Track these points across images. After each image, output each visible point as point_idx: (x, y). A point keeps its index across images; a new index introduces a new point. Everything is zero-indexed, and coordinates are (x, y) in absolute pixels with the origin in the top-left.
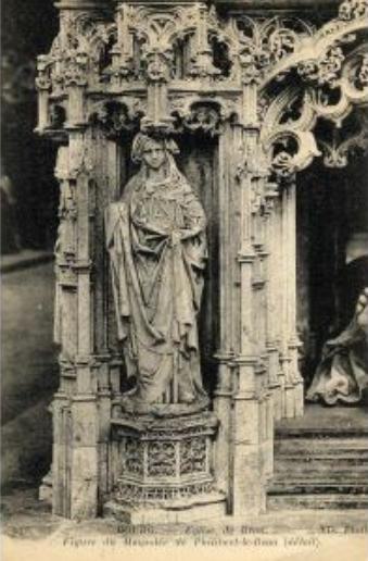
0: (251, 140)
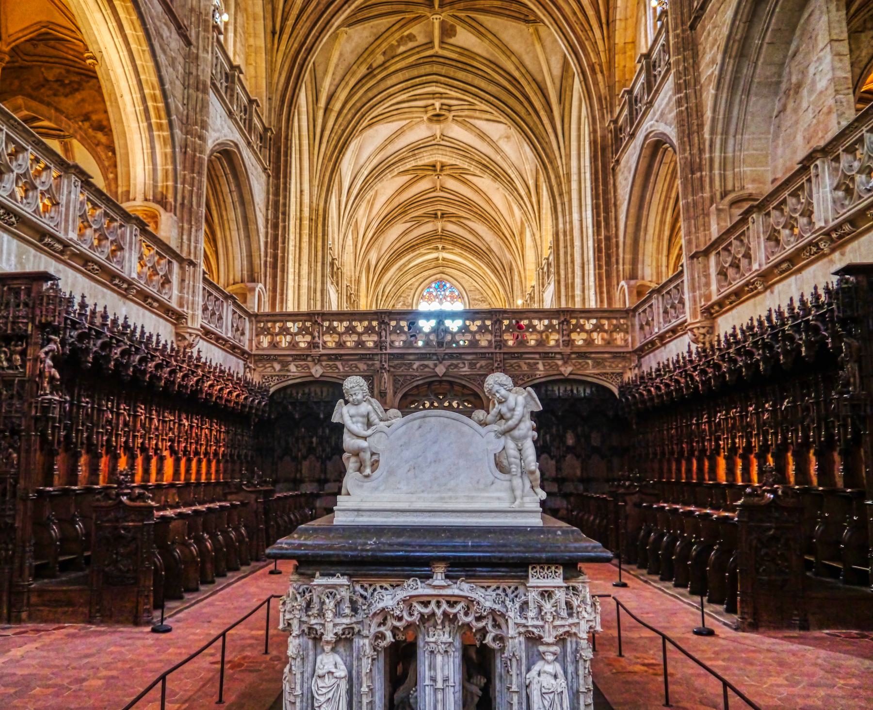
0: (366, 641)
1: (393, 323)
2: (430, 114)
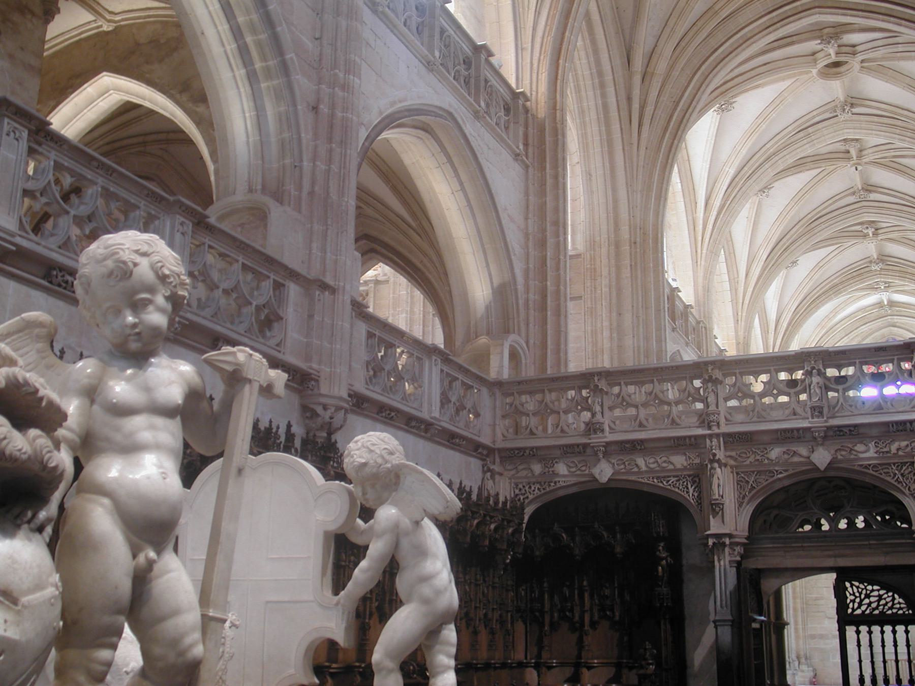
1: (731, 380)
2: (822, 64)
